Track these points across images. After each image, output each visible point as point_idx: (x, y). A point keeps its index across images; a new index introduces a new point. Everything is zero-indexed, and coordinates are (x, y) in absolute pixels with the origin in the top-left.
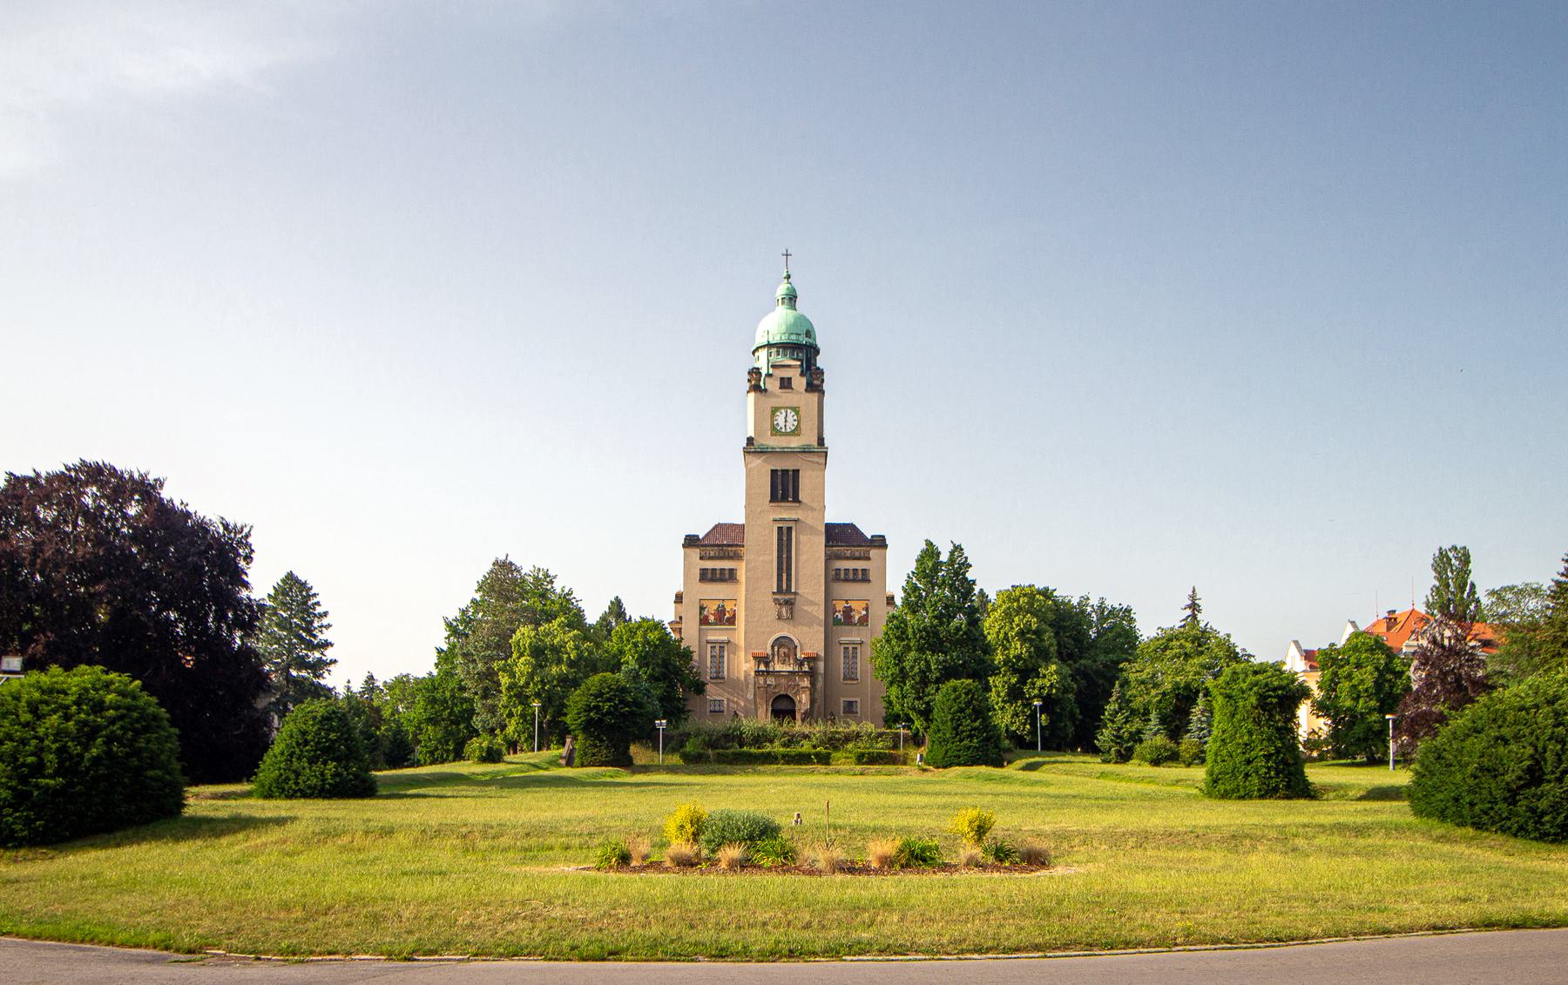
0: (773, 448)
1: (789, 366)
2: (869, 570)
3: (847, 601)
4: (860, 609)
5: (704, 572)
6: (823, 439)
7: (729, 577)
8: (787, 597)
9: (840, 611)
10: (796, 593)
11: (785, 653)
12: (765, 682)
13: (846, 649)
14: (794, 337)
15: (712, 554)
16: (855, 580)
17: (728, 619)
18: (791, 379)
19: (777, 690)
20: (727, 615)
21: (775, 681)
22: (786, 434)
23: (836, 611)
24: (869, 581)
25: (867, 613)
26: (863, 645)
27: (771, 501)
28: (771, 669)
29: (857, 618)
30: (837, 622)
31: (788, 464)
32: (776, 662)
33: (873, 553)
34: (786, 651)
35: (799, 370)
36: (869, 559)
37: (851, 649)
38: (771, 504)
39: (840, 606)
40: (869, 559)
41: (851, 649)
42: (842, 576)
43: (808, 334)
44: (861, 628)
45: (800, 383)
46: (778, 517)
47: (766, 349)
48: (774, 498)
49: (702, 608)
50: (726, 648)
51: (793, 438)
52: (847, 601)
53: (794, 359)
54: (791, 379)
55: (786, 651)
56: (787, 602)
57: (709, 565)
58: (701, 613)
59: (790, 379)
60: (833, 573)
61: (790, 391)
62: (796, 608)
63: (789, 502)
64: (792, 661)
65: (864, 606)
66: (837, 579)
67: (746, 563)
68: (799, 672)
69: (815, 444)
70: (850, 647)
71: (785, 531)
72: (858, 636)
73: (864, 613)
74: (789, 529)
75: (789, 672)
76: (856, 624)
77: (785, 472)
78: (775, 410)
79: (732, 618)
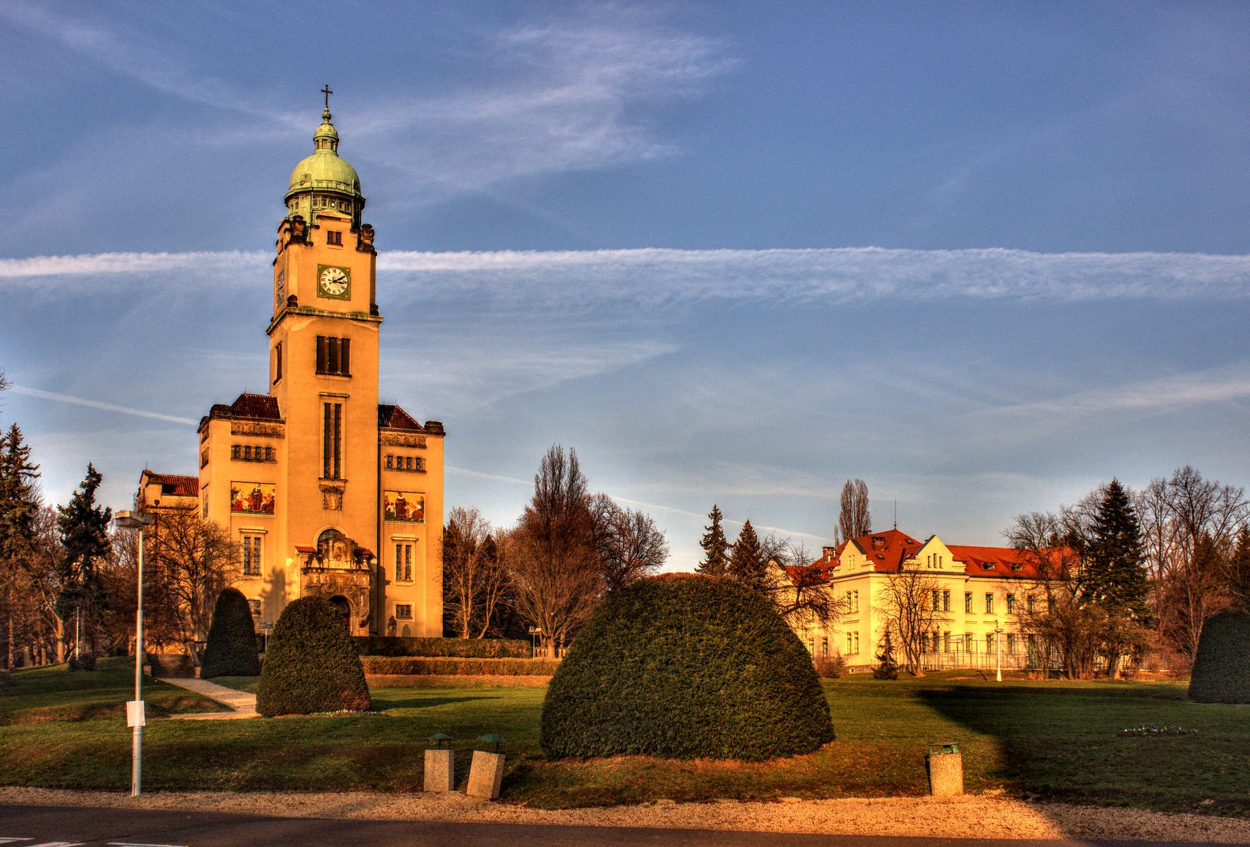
0: (320, 311)
1: (339, 219)
2: (425, 460)
3: (399, 492)
4: (415, 503)
5: (236, 449)
6: (377, 307)
7: (265, 456)
8: (336, 484)
9: (392, 504)
10: (346, 481)
13: (399, 546)
14: (342, 187)
15: (246, 429)
16: (409, 470)
17: (265, 507)
18: (340, 233)
20: (264, 502)
22: (333, 297)
23: (388, 504)
24: (424, 472)
27: (317, 373)
28: (326, 566)
29: (411, 512)
30: (389, 516)
31: (339, 331)
32: (331, 558)
33: (430, 440)
34: (342, 545)
35: (349, 226)
36: (424, 447)
38: (319, 376)
39: (393, 498)
40: (424, 447)
42: (395, 464)
43: (357, 186)
44: (416, 524)
45: (350, 240)
46: (325, 391)
47: (309, 197)
48: (320, 369)
49: (234, 492)
50: (262, 540)
51: (342, 303)
52: (399, 492)
53: (341, 212)
54: (340, 233)
56: (337, 491)
57: (243, 440)
58: (232, 499)
59: (339, 234)
60: (386, 460)
61: (340, 247)
62: (346, 497)
63: (338, 375)
65: (419, 499)
66: (389, 467)
67: (289, 442)
68: (357, 570)
69: (366, 309)
71: (333, 408)
72: (412, 533)
73: (419, 507)
74: (338, 406)
75: (345, 570)
76: (409, 520)
77: (333, 340)
78: (322, 269)
79: (269, 505)
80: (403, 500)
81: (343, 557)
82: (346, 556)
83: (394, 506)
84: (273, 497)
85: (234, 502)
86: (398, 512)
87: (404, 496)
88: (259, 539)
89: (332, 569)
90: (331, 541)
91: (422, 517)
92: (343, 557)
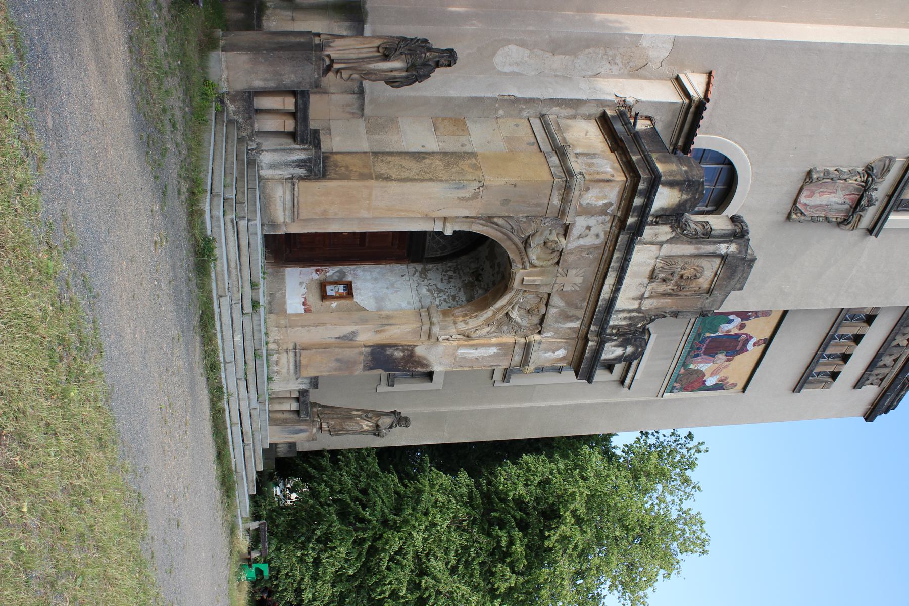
9: (742, 326)
12: (588, 211)
16: (815, 360)
19: (534, 254)
21: (581, 249)
26: (615, 387)
32: (667, 250)
52: (768, 343)
73: (710, 381)
80: (744, 349)
82: (664, 295)
83: (736, 331)
87: (753, 351)
90: (733, 248)
92: (663, 288)
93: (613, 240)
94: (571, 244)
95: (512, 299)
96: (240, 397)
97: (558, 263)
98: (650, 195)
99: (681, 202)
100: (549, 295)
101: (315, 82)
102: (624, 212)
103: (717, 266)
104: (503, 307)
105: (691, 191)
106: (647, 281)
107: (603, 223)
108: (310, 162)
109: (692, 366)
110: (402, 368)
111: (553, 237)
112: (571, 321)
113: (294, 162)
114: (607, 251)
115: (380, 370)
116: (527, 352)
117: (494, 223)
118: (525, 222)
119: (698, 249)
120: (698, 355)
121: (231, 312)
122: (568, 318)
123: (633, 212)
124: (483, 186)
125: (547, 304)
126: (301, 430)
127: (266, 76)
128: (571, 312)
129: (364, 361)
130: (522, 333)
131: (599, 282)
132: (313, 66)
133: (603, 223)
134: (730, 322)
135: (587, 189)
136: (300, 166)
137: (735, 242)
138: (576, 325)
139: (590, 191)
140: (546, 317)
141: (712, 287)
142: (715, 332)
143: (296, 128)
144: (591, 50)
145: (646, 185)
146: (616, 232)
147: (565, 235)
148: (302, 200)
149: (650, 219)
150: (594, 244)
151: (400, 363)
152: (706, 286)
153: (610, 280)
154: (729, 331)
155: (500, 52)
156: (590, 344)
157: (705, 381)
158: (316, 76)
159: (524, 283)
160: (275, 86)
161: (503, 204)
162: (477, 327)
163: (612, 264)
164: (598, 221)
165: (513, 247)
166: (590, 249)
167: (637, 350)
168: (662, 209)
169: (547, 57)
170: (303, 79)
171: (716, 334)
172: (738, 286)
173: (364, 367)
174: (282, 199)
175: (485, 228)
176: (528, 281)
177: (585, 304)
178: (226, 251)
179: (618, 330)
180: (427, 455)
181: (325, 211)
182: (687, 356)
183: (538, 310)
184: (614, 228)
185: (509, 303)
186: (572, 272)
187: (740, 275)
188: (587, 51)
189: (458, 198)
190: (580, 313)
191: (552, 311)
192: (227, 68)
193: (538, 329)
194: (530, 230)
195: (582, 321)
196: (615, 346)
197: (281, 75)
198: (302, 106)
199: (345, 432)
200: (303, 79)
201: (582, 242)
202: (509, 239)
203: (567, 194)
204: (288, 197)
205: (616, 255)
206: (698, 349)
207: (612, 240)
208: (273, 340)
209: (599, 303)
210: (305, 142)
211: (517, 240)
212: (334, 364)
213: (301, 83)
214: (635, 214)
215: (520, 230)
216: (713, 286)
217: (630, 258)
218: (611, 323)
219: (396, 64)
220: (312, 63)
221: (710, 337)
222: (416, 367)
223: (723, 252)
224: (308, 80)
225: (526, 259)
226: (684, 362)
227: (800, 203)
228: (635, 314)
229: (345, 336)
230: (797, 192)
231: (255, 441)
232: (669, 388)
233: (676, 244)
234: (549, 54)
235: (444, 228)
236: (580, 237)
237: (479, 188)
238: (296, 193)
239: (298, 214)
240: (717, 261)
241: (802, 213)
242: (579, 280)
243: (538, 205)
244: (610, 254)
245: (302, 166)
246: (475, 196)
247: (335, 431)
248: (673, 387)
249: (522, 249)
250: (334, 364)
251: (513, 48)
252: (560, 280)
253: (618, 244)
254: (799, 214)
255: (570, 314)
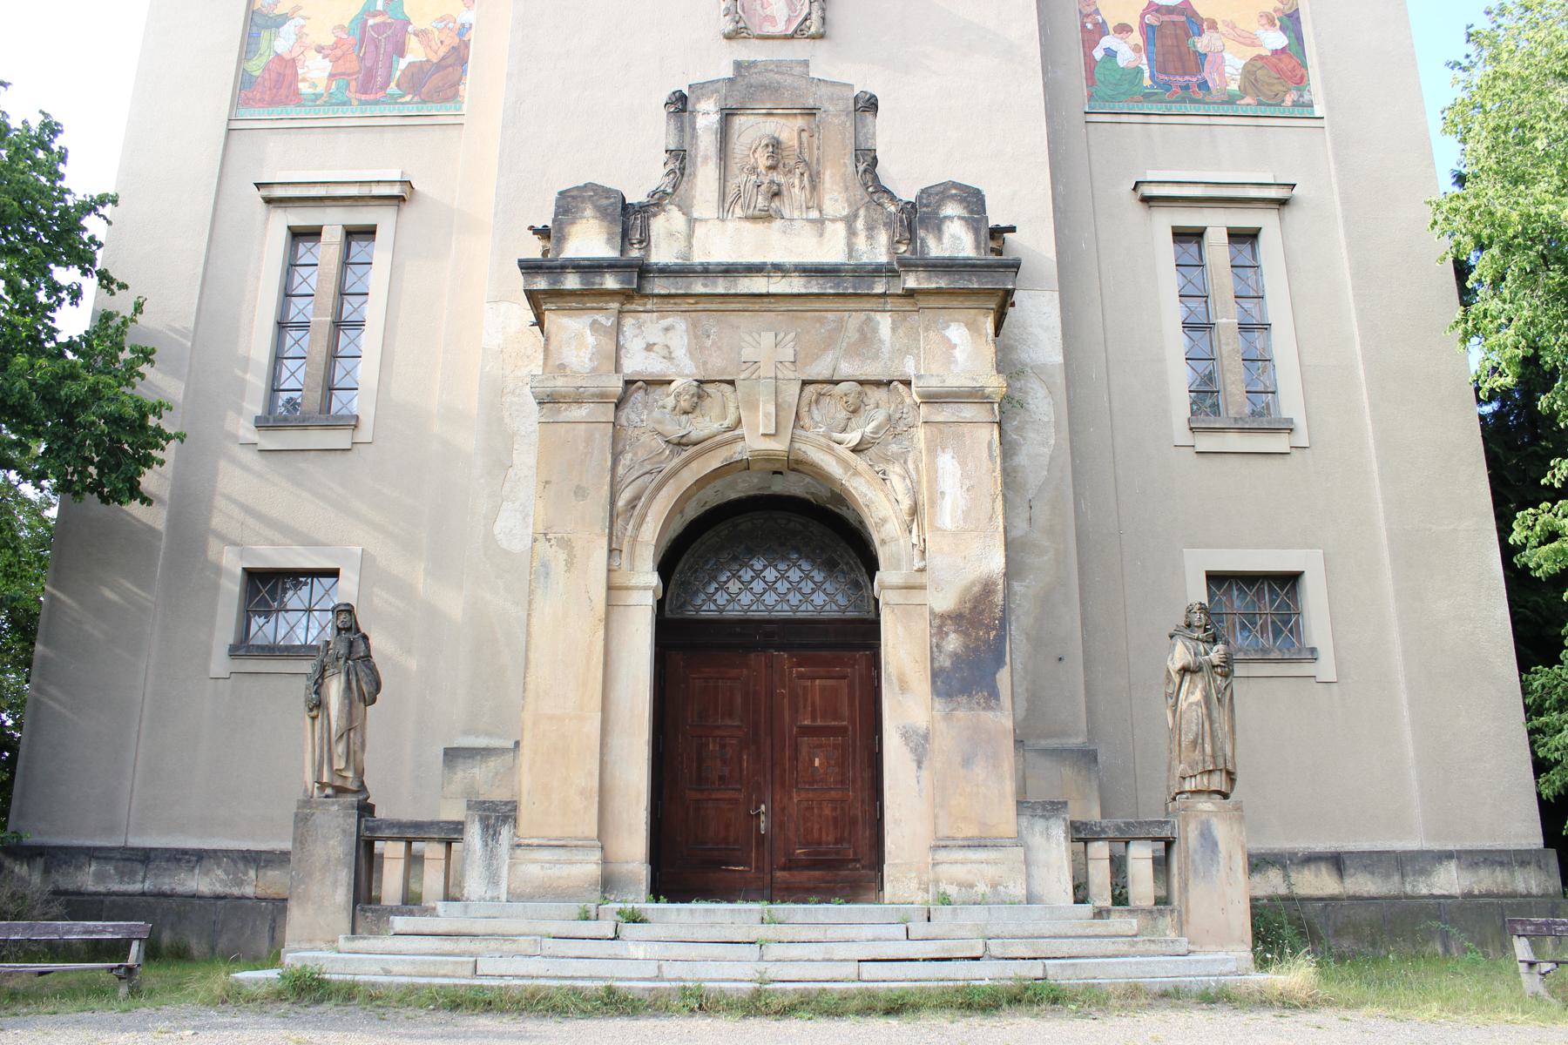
9: (1123, 29)
11: (776, 145)
17: (417, 80)
20: (416, 52)
21: (696, 350)
23: (1101, 29)
25: (1299, 38)
28: (662, 254)
37: (1216, 239)
41: (1216, 239)
55: (787, 130)
64: (835, 201)
70: (1217, 224)
73: (1276, 40)
79: (440, 66)
81: (797, 191)
83: (1136, 38)
84: (464, 29)
85: (256, 66)
86: (1159, 67)
88: (369, 232)
89: (706, 271)
91: (1301, 81)
92: (797, 191)
93: (672, 301)
94: (684, 370)
95: (820, 447)
96: (820, 958)
97: (731, 383)
98: (556, 268)
99: (598, 215)
100: (805, 383)
101: (346, 808)
102: (608, 298)
103: (752, 118)
104: (841, 461)
105: (577, 207)
106: (778, 223)
107: (640, 327)
108: (488, 818)
109: (1234, 87)
110: (993, 634)
111: (670, 402)
112: (875, 330)
113: (487, 845)
114: (700, 307)
115: (997, 676)
116: (946, 398)
117: (632, 504)
118: (635, 454)
119: (706, 159)
120: (1203, 85)
121: (557, 957)
122: (866, 337)
123: (593, 284)
124: (545, 534)
125: (837, 383)
126: (1202, 834)
127: (329, 883)
128: (851, 334)
129: (972, 709)
130: (911, 414)
131: (770, 303)
132: (318, 813)
133: (640, 327)
134: (1111, 54)
135: (562, 367)
136: (494, 834)
137: (694, 106)
138: (884, 322)
139: (565, 361)
140: (863, 378)
141: (799, 111)
142: (1139, 71)
143: (440, 840)
144: (506, 414)
145: (538, 280)
146: (655, 300)
147: (670, 382)
148: (556, 833)
149: (635, 253)
150: (687, 331)
151: (977, 639)
152: (800, 122)
153: (758, 285)
154: (1136, 49)
155: (505, 545)
156: (911, 282)
157: (1275, 52)
158: (336, 807)
159: (773, 432)
160: (346, 870)
161: (584, 497)
162: (889, 500)
163: (721, 290)
164: (636, 336)
165: (694, 465)
166: (697, 333)
167: (953, 196)
168: (609, 240)
169: (516, 475)
170: (338, 827)
171: (1145, 68)
172: (798, 70)
173: (988, 708)
174: (548, 865)
175: (649, 519)
176: (766, 426)
177: (830, 315)
178: (414, 955)
179: (898, 242)
180: (1515, 560)
181: (582, 793)
182: (1207, 103)
183: (846, 395)
184: (649, 307)
185: (830, 450)
186: (748, 353)
187: (771, 74)
188: (507, 420)
189: (568, 570)
190: (854, 321)
191: (846, 369)
192: (310, 941)
193: (896, 387)
194: (653, 442)
195: (872, 311)
196: (939, 239)
197: (329, 860)
198: (395, 830)
199: (1207, 740)
200: (338, 827)
201: (680, 352)
202: (674, 473)
203: (564, 397)
204: (546, 855)
205: (699, 287)
206: (1187, 88)
207: (675, 304)
208: (920, 893)
209: (817, 291)
210: (460, 827)
211: (676, 461)
212: (980, 771)
213: (344, 831)
214: (597, 280)
215: (655, 460)
216: (795, 111)
217: (702, 264)
218: (883, 258)
219: (335, 689)
220: (313, 814)
221: (1152, 77)
222: (992, 604)
223: (715, 118)
224: (341, 820)
225: (718, 438)
226: (1223, 103)
227: (787, 29)
228: (860, 224)
229: (914, 750)
230: (770, 42)
231: (1020, 933)
232: (1297, 112)
233: (694, 197)
234: (511, 472)
235: (645, 588)
236: (669, 357)
237: (549, 540)
238: (535, 841)
239: (586, 839)
240: (739, 122)
241: (806, 19)
242: (768, 339)
243: (589, 440)
244: (703, 299)
245: (495, 831)
246: (566, 544)
247: (1204, 761)
248: (1295, 104)
249: (692, 450)
250: (980, 771)
251: (497, 528)
252: (767, 371)
253: (673, 291)
254: (808, 23)
255: (857, 335)
